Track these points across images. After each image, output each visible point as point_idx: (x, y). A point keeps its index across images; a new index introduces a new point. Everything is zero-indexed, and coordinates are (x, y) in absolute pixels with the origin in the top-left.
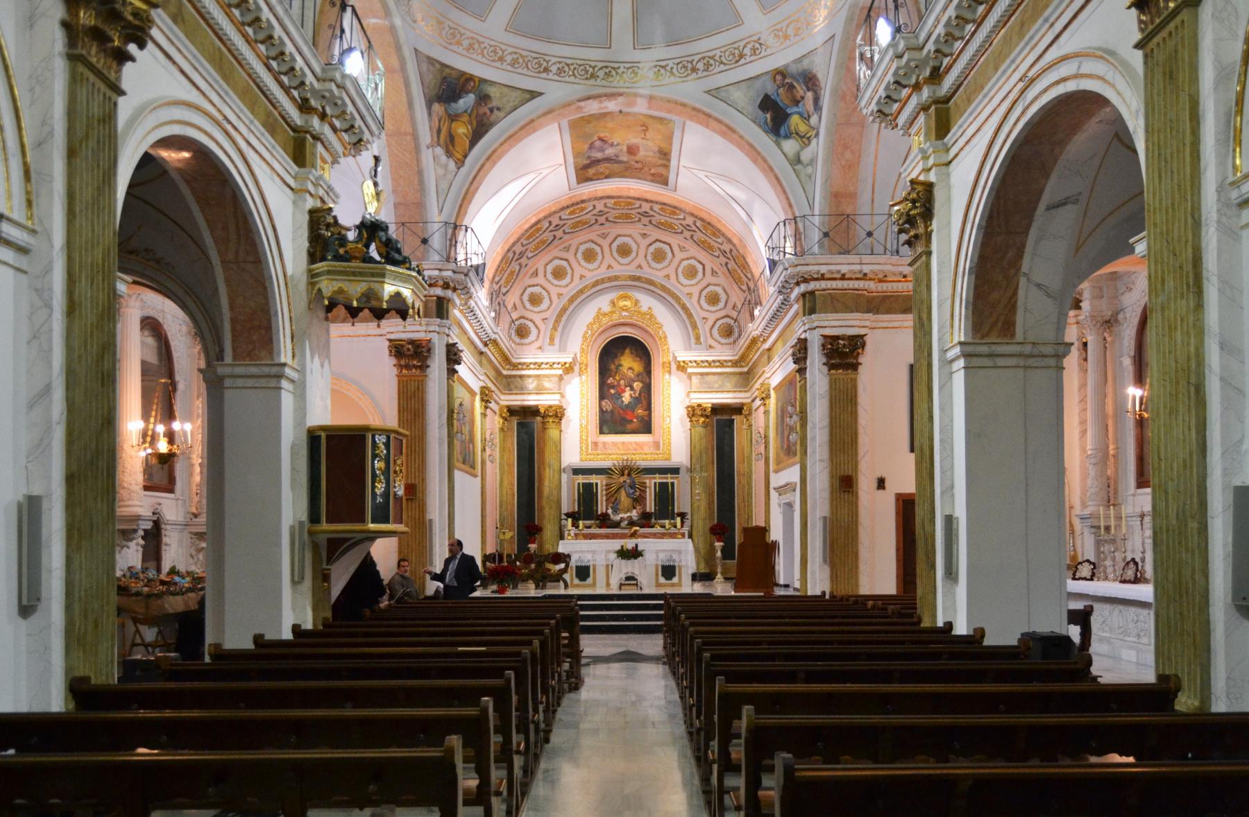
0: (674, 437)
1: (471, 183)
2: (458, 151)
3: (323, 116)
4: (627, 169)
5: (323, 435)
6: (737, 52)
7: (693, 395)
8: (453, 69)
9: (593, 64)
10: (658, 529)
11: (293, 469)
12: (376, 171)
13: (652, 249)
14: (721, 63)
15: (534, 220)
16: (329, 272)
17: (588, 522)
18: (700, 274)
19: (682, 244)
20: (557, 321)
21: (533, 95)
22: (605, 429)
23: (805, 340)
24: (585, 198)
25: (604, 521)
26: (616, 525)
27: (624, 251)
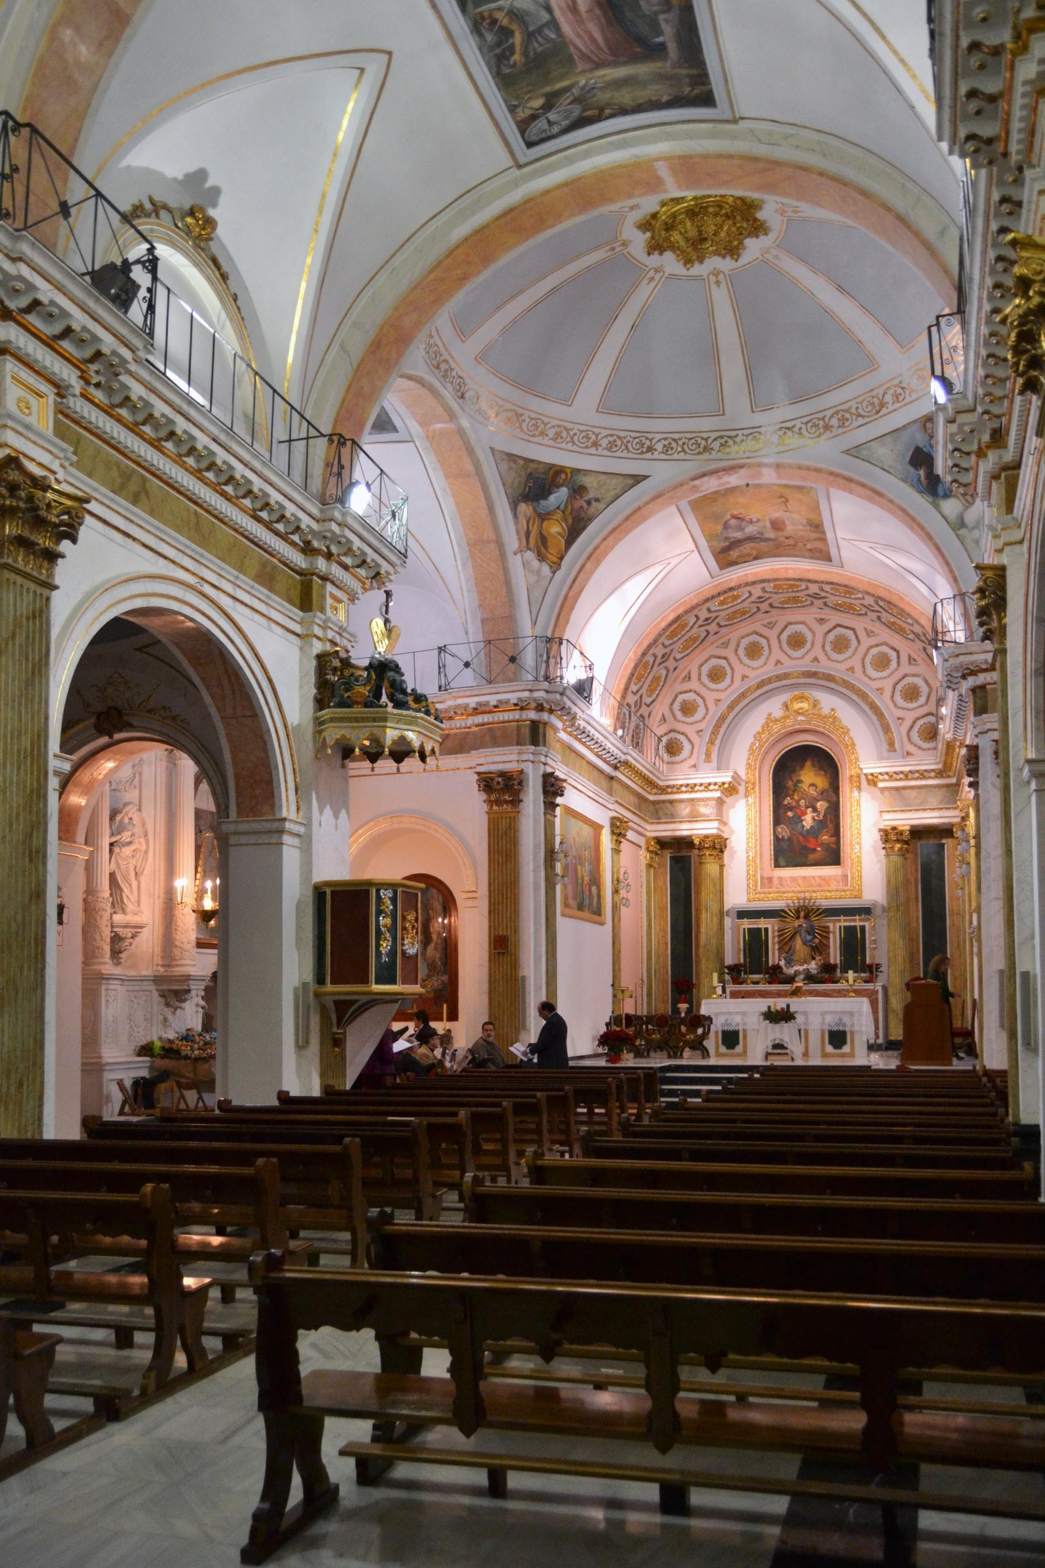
0: (866, 869)
1: (571, 587)
2: (552, 555)
3: (329, 556)
4: (778, 547)
5: (328, 891)
6: (876, 401)
9: (705, 435)
10: (842, 985)
11: (299, 928)
12: (387, 607)
13: (831, 637)
14: (859, 415)
15: (672, 617)
16: (332, 720)
17: (756, 977)
18: (894, 663)
19: (869, 628)
20: (715, 733)
21: (638, 479)
22: (782, 861)
23: (976, 747)
24: (732, 584)
25: (775, 975)
26: (790, 980)
27: (797, 642)
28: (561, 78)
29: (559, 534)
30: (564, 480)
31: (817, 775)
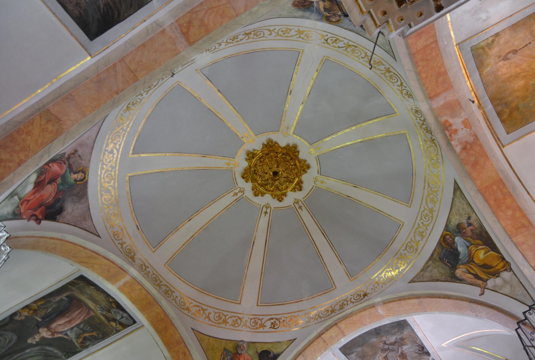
8: (435, 250)
21: (457, 188)
28: (100, 319)
29: (485, 254)
30: (451, 237)
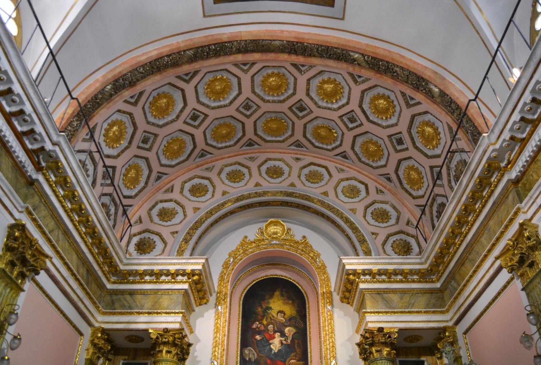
7: (369, 318)
27: (275, 173)
31: (285, 303)
